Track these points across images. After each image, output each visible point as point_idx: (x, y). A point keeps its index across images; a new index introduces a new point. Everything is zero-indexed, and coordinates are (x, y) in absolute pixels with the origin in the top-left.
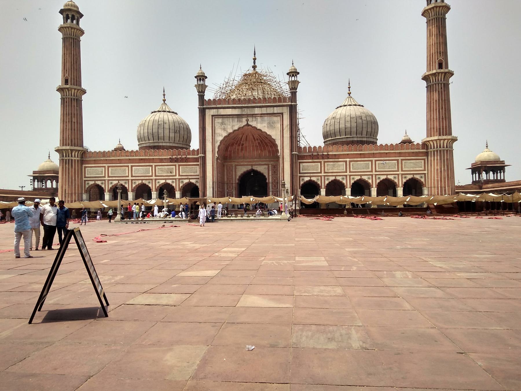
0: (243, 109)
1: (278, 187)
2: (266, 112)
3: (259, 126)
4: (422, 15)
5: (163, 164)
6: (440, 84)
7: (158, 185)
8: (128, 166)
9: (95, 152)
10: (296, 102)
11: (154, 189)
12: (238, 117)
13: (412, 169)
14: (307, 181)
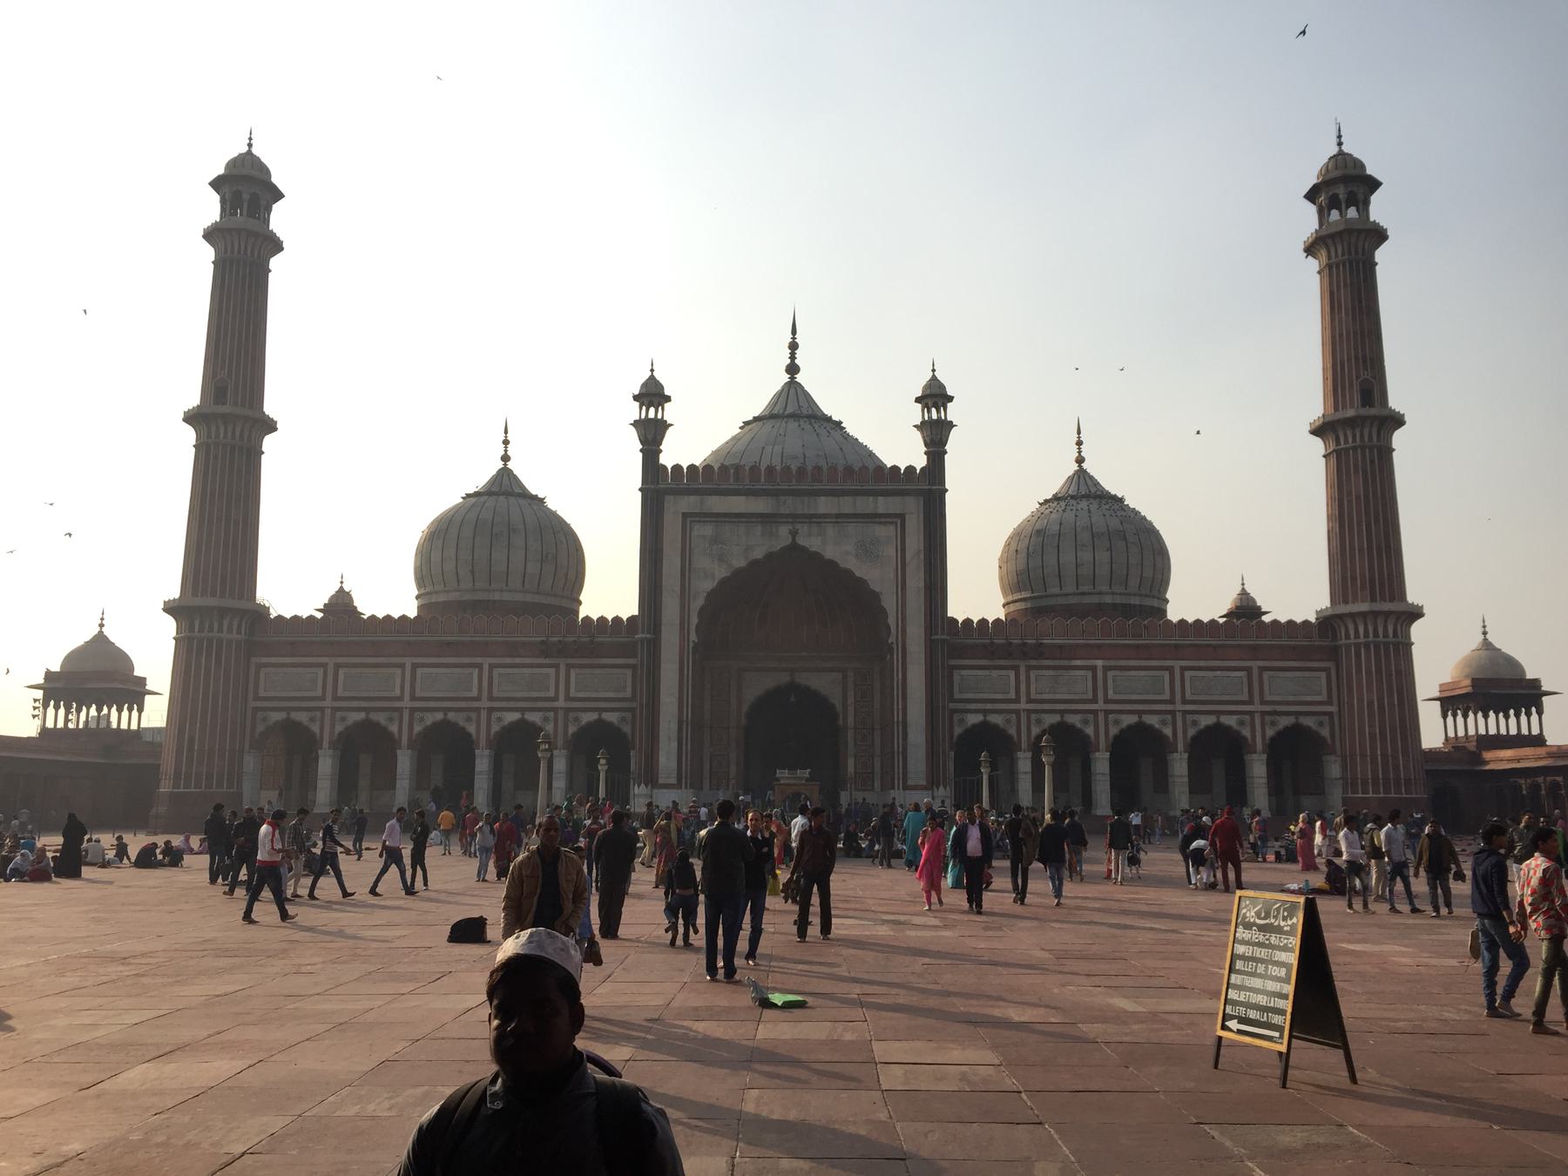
1: (873, 740)
2: (852, 512)
3: (830, 552)
4: (1310, 250)
5: (518, 660)
6: (1367, 450)
7: (495, 728)
8: (402, 666)
9: (295, 617)
11: (483, 742)
13: (1291, 698)
14: (974, 726)
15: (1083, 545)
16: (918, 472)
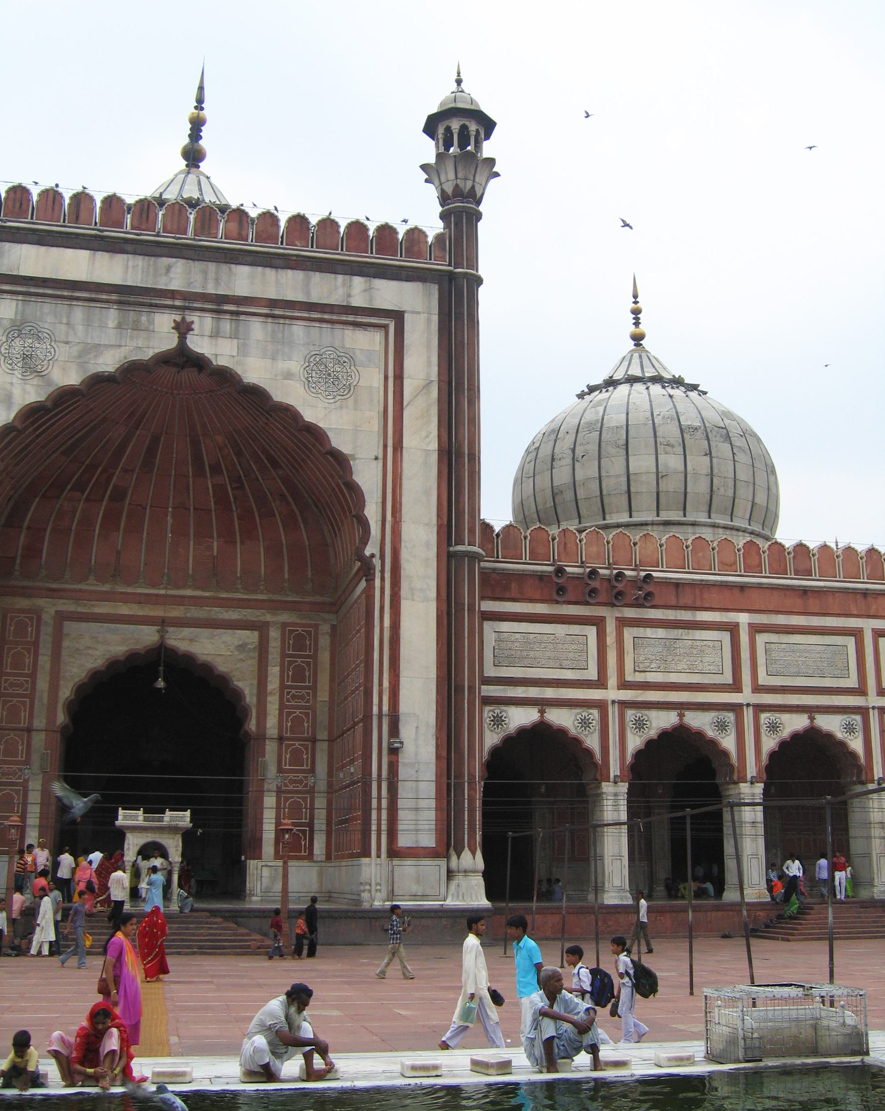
0: (166, 261)
2: (300, 297)
10: (473, 261)
12: (129, 303)
14: (524, 733)
15: (668, 445)
16: (430, 239)
